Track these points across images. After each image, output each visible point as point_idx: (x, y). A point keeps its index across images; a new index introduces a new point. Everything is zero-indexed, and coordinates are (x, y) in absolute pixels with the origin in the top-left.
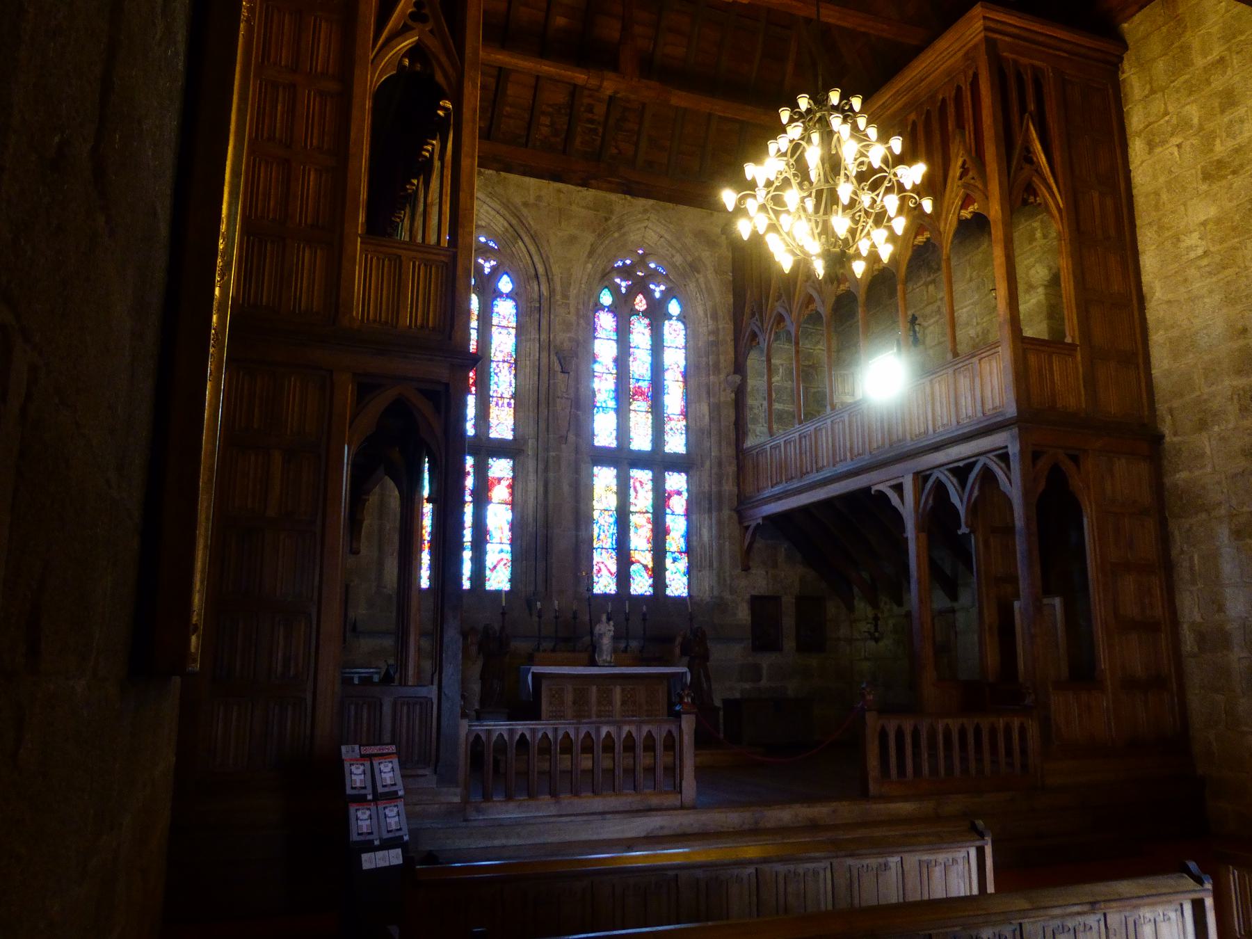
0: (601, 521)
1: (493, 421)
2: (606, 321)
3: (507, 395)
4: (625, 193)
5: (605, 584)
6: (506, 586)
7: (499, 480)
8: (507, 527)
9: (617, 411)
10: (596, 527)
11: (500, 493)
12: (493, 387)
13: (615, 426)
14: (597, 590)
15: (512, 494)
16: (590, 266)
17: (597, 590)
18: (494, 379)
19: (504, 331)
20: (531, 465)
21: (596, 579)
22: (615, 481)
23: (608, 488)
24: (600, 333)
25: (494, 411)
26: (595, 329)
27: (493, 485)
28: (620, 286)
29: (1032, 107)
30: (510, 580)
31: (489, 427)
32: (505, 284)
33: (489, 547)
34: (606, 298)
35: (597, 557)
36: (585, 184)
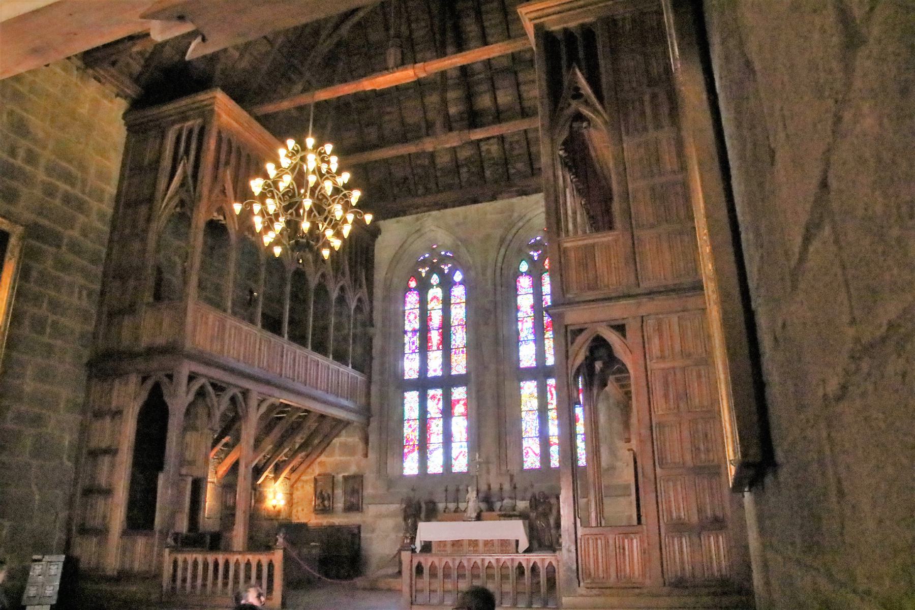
0: (527, 419)
1: (453, 364)
2: (525, 283)
3: (461, 346)
4: (520, 195)
5: (532, 461)
6: (464, 469)
7: (458, 401)
8: (464, 431)
9: (535, 341)
10: (524, 424)
11: (459, 409)
12: (453, 343)
13: (534, 352)
14: (526, 466)
15: (466, 409)
16: (503, 251)
17: (526, 466)
18: (453, 337)
19: (458, 306)
20: (474, 389)
21: (525, 459)
22: (536, 390)
23: (531, 395)
24: (521, 291)
25: (454, 358)
26: (517, 290)
27: (455, 405)
28: (533, 256)
29: (581, 55)
30: (467, 465)
31: (451, 368)
32: (458, 277)
33: (453, 445)
34: (524, 267)
35: (525, 444)
36: (494, 198)
